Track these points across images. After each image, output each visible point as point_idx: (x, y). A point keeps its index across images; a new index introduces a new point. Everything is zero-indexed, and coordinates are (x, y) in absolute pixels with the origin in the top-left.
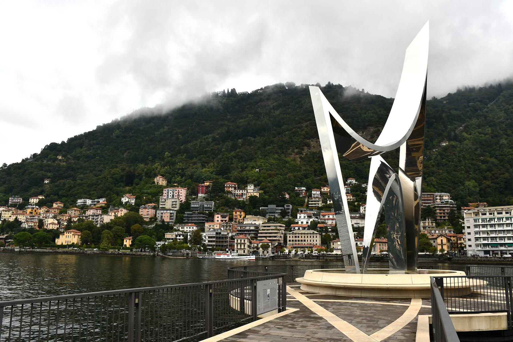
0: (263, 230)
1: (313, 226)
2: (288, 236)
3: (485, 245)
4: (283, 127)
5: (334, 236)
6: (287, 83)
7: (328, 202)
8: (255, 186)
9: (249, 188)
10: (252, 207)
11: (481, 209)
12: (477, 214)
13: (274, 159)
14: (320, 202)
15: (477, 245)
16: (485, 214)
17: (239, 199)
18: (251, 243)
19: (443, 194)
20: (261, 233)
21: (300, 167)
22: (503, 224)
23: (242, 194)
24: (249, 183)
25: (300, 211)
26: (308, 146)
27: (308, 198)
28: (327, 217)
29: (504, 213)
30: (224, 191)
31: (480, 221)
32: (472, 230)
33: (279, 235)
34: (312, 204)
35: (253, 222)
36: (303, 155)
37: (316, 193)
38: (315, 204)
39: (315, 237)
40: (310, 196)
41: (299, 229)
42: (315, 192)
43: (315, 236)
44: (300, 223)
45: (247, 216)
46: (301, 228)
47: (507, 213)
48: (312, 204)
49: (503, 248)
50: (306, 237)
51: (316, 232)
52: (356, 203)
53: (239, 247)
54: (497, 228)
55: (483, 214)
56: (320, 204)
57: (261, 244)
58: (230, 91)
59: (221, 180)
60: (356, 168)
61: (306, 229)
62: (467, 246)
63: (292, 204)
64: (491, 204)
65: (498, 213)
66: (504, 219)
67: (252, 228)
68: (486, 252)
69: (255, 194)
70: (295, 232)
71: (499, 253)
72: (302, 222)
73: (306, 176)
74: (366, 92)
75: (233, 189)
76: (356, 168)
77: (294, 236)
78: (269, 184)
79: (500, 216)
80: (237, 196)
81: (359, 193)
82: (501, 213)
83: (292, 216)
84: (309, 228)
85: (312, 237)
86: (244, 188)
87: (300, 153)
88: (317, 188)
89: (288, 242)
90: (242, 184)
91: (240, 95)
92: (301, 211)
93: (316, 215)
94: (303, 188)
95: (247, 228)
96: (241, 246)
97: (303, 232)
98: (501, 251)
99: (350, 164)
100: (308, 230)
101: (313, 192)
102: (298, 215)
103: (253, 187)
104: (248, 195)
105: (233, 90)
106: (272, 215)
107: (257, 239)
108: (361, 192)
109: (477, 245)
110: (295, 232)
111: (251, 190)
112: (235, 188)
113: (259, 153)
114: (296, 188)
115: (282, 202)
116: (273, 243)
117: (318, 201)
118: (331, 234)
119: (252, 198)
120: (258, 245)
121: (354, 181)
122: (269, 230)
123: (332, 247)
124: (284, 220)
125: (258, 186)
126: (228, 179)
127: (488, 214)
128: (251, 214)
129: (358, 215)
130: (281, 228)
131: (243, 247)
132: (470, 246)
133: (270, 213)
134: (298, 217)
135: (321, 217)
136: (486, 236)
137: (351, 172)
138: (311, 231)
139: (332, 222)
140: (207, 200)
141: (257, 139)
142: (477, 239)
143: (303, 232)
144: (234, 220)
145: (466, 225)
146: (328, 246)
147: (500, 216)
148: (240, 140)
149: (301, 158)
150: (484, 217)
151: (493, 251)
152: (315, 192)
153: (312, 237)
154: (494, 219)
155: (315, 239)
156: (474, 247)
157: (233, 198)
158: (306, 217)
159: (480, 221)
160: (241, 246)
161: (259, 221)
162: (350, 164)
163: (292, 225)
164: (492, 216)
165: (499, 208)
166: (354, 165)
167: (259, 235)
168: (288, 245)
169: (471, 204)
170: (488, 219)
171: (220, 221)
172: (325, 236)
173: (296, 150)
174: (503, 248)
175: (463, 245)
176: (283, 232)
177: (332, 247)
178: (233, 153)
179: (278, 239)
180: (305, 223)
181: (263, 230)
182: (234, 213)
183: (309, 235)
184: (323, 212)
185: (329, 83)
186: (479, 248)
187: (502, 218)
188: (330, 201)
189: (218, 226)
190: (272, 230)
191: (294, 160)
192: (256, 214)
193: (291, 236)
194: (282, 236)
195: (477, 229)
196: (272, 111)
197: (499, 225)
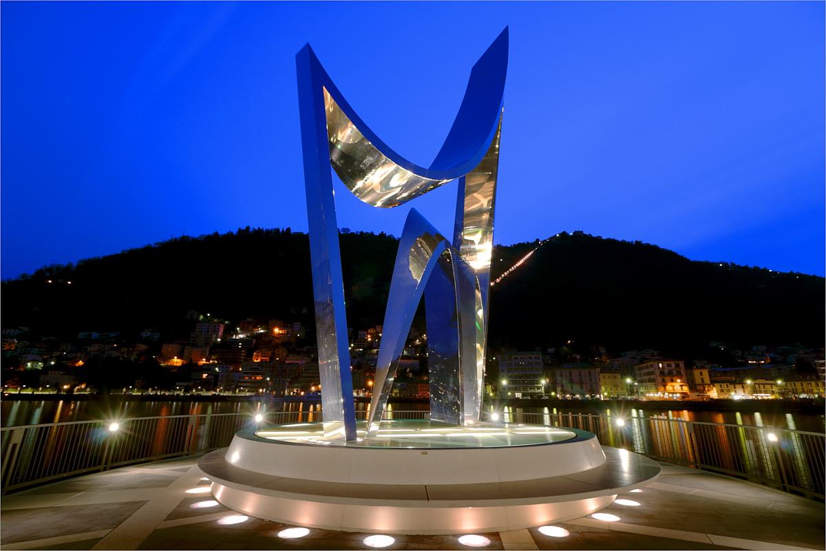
8: (302, 325)
58: (285, 230)
98: (531, 393)
105: (288, 230)
192: (299, 353)
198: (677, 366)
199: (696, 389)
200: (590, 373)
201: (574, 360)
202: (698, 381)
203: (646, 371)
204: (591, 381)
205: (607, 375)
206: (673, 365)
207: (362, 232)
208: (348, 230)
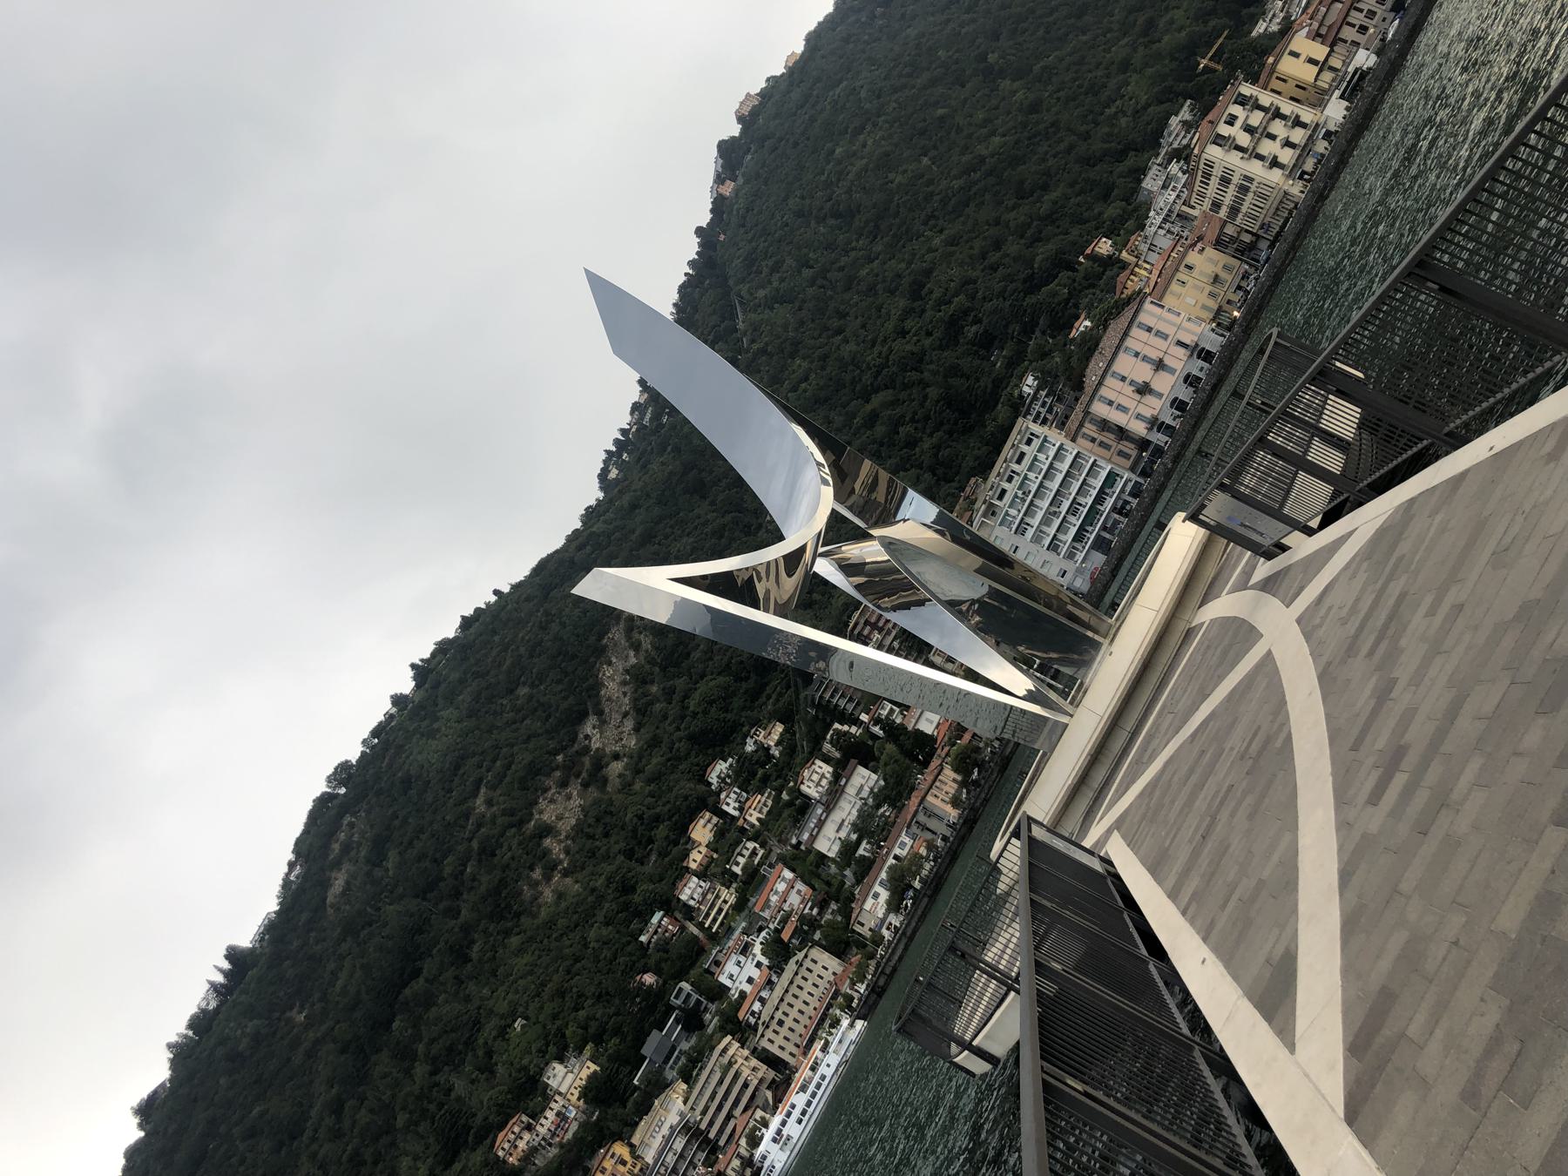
0: (704, 1113)
1: (779, 953)
2: (764, 1044)
3: (1079, 537)
4: (447, 870)
5: (839, 911)
6: (329, 780)
7: (737, 870)
8: (561, 1059)
9: (553, 1083)
11: (985, 492)
12: (991, 511)
13: (520, 951)
14: (724, 893)
15: (1070, 556)
16: (1004, 492)
17: (569, 1135)
20: (711, 1124)
21: (593, 890)
22: (1051, 466)
23: (558, 1114)
24: (541, 1072)
25: (714, 969)
26: (547, 830)
27: (691, 919)
28: (774, 899)
29: (1025, 448)
33: (746, 1072)
34: (715, 920)
35: (665, 1131)
36: (561, 862)
37: (690, 891)
38: (720, 910)
40: (689, 912)
41: (763, 1001)
43: (808, 964)
44: (748, 988)
45: (635, 1140)
46: (764, 994)
47: (1029, 442)
48: (715, 920)
49: (1109, 503)
50: (797, 992)
52: (785, 796)
54: (1054, 485)
55: (1001, 498)
56: (729, 896)
58: (226, 965)
59: (477, 1157)
60: (692, 738)
61: (774, 978)
63: (681, 975)
64: (984, 468)
65: (1019, 462)
67: (679, 1144)
68: (1100, 545)
69: (585, 1073)
70: (765, 1017)
72: (750, 980)
73: (627, 888)
74: (506, 589)
75: (527, 1136)
76: (692, 738)
77: (774, 1025)
78: (582, 1014)
79: (1027, 461)
80: (554, 1135)
81: (760, 772)
82: (1023, 455)
83: (712, 1000)
84: (777, 967)
85: (807, 974)
87: (551, 868)
88: (680, 877)
89: (785, 1056)
90: (530, 1094)
91: (262, 940)
92: (717, 963)
93: (755, 927)
94: (655, 920)
95: (670, 1159)
97: (778, 991)
98: (1114, 509)
99: (671, 749)
100: (779, 975)
101: (683, 897)
102: (723, 979)
103: (559, 1069)
104: (574, 1099)
105: (233, 954)
106: (678, 1058)
108: (763, 766)
109: (1070, 556)
110: (765, 1017)
111: (567, 1079)
112: (529, 1128)
113: (472, 987)
114: (643, 938)
115: (655, 1008)
116: (759, 1101)
117: (718, 897)
118: (828, 916)
119: (593, 1092)
120: (739, 1156)
121: (721, 767)
123: (868, 934)
124: (710, 1031)
125: (565, 1048)
127: (1006, 485)
128: (637, 1124)
129: (819, 811)
130: (730, 1052)
133: (666, 1061)
134: (728, 983)
135: (766, 914)
136: (1057, 523)
137: (693, 759)
138: (791, 967)
139: (799, 892)
141: (429, 967)
142: (1053, 547)
143: (778, 991)
146: (861, 943)
148: (395, 1025)
149: (566, 873)
150: (1008, 498)
151: (1104, 528)
152: (687, 891)
153: (807, 974)
154: (1026, 478)
155: (817, 969)
156: (1070, 567)
157: (554, 1151)
158: (742, 959)
161: (673, 1108)
162: (671, 749)
163: (741, 1015)
164: (1017, 480)
165: (1007, 451)
166: (680, 740)
167: (712, 1135)
172: (825, 936)
173: (537, 874)
174: (1109, 503)
176: (746, 1052)
177: (868, 934)
178: (420, 1070)
179: (756, 1082)
180: (755, 973)
181: (704, 1113)
183: (798, 980)
184: (756, 903)
185: (413, 666)
186: (1080, 556)
188: (737, 864)
190: (721, 1082)
191: (560, 896)
192: (645, 1108)
193: (769, 1034)
194: (754, 1062)
195: (1030, 533)
196: (378, 873)
197: (1048, 475)
198: (1242, 101)
199: (1324, 92)
201: (1090, 344)
202: (1308, 73)
203: (1214, 182)
204: (1165, 337)
205: (1175, 287)
206: (1236, 110)
207: (376, 733)
208: (344, 767)
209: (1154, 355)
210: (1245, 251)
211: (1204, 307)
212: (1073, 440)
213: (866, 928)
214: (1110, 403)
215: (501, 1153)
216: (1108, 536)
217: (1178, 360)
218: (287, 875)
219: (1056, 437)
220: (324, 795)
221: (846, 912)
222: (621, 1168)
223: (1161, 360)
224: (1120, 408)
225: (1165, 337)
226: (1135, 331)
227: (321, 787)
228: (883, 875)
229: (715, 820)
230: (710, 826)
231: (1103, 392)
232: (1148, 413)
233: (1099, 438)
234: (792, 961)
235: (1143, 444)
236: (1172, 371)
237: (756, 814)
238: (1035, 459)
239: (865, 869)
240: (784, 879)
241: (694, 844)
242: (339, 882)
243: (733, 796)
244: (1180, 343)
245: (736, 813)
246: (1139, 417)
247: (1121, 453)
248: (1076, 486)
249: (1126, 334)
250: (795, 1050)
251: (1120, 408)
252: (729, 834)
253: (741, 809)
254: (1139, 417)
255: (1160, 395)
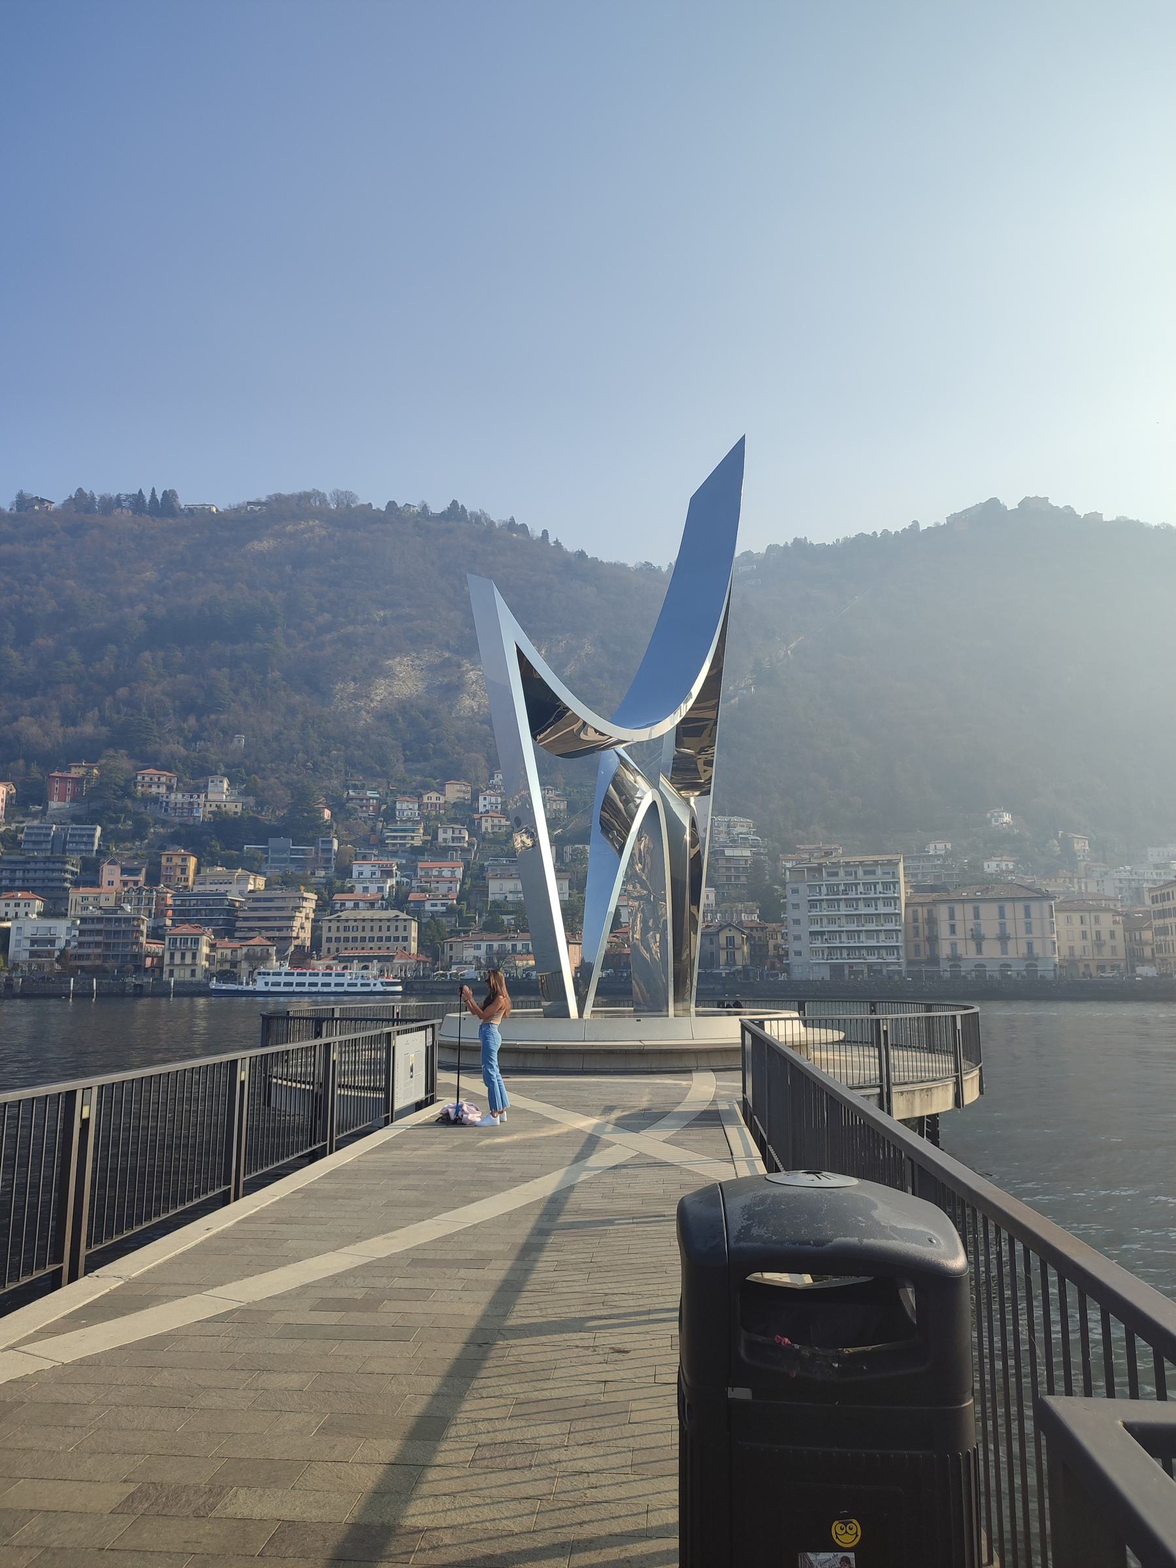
1: (399, 901)
2: (325, 925)
10: (222, 841)
15: (814, 951)
16: (836, 874)
18: (213, 947)
19: (735, 819)
20: (246, 919)
30: (131, 796)
31: (824, 889)
32: (803, 913)
34: (395, 838)
37: (406, 807)
39: (401, 928)
41: (356, 906)
42: (405, 806)
43: (401, 925)
44: (359, 888)
46: (361, 904)
48: (395, 838)
51: (403, 916)
53: (177, 960)
55: (829, 874)
57: (245, 950)
58: (159, 497)
62: (792, 955)
65: (866, 873)
66: (880, 888)
68: (836, 969)
70: (344, 915)
71: (866, 971)
72: (366, 889)
75: (163, 790)
77: (342, 925)
86: (202, 789)
89: (325, 945)
92: (364, 858)
96: (183, 957)
97: (368, 914)
101: (398, 806)
102: (356, 870)
104: (208, 809)
105: (169, 496)
107: (232, 937)
110: (344, 915)
111: (221, 794)
112: (169, 788)
117: (413, 831)
122: (269, 909)
126: (151, 760)
130: (305, 904)
131: (188, 960)
132: (799, 953)
134: (355, 874)
138: (391, 913)
139: (450, 889)
140: (76, 819)
144: (163, 879)
145: (792, 899)
147: (870, 879)
150: (833, 880)
152: (405, 806)
154: (856, 885)
158: (378, 874)
159: (824, 889)
160: (183, 957)
163: (337, 897)
167: (238, 924)
168: (324, 952)
169: (802, 847)
170: (842, 888)
171: (117, 884)
174: (872, 959)
175: (782, 952)
176: (312, 916)
180: (373, 888)
182: (164, 860)
187: (875, 884)
189: (112, 898)
193: (334, 925)
194: (308, 925)
197: (868, 902)
200: (1028, 914)
204: (1029, 930)
205: (1076, 917)
209: (1010, 930)
210: (1135, 956)
211: (1071, 948)
212: (907, 905)
213: (450, 953)
214: (952, 917)
215: (139, 778)
216: (846, 972)
217: (1016, 950)
218: (249, 503)
219: (903, 892)
220: (324, 495)
221: (455, 933)
222: (178, 871)
223: (1009, 938)
224: (953, 929)
225: (1029, 930)
226: (1020, 906)
227: (327, 490)
228: (496, 945)
229: (468, 796)
230: (461, 795)
231: (958, 908)
232: (961, 950)
233: (920, 924)
234: (396, 912)
235: (934, 960)
236: (1004, 951)
237: (489, 824)
238: (875, 884)
239: (494, 927)
240: (453, 872)
241: (441, 790)
242: (264, 545)
243: (493, 800)
244: (1030, 946)
245: (481, 809)
246: (954, 945)
247: (917, 947)
248: (872, 927)
249: (1013, 900)
250: (333, 950)
251: (953, 929)
252: (465, 814)
253: (487, 812)
254: (954, 945)
255: (979, 950)
